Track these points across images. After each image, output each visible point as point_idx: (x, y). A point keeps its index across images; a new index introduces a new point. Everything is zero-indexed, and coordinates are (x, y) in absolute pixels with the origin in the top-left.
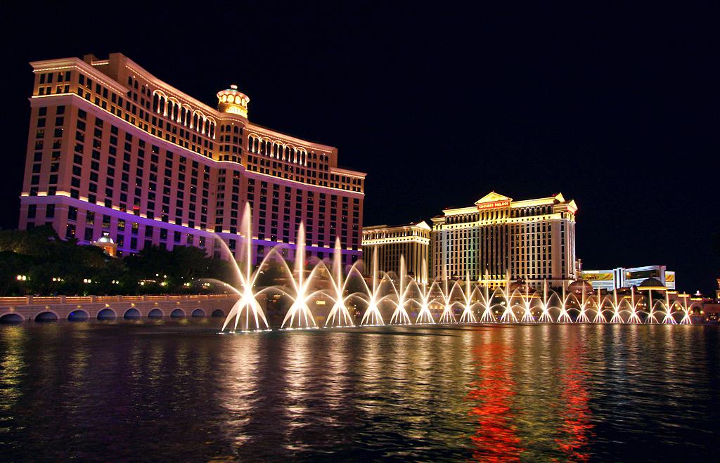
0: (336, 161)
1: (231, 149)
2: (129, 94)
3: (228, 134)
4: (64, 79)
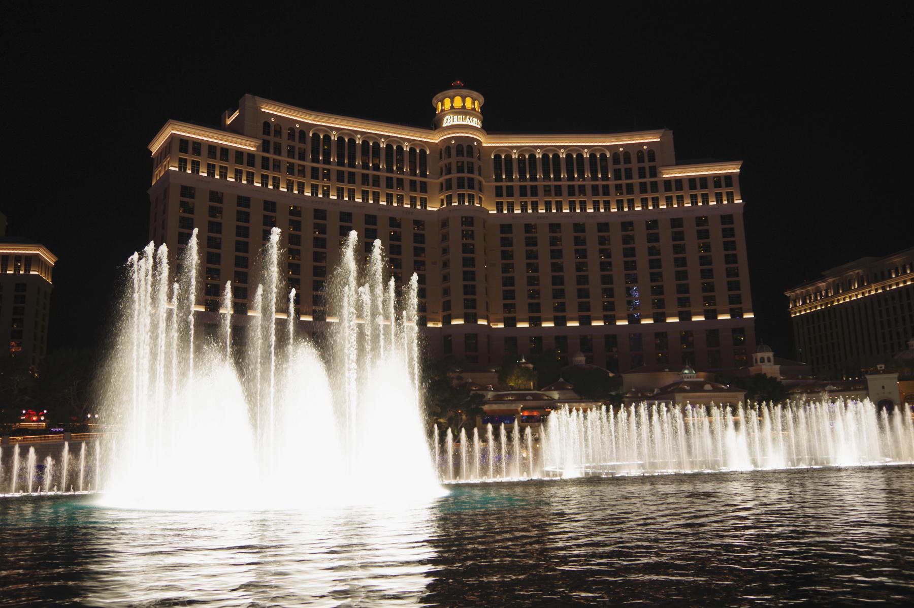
0: (673, 153)
1: (454, 184)
2: (265, 147)
3: (448, 160)
4: (167, 152)
